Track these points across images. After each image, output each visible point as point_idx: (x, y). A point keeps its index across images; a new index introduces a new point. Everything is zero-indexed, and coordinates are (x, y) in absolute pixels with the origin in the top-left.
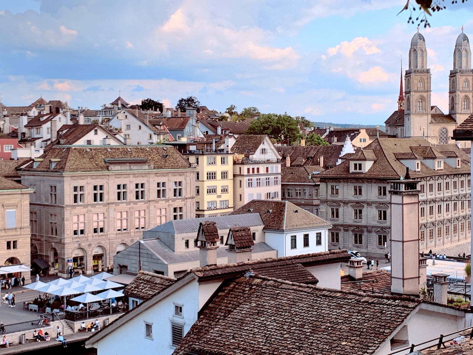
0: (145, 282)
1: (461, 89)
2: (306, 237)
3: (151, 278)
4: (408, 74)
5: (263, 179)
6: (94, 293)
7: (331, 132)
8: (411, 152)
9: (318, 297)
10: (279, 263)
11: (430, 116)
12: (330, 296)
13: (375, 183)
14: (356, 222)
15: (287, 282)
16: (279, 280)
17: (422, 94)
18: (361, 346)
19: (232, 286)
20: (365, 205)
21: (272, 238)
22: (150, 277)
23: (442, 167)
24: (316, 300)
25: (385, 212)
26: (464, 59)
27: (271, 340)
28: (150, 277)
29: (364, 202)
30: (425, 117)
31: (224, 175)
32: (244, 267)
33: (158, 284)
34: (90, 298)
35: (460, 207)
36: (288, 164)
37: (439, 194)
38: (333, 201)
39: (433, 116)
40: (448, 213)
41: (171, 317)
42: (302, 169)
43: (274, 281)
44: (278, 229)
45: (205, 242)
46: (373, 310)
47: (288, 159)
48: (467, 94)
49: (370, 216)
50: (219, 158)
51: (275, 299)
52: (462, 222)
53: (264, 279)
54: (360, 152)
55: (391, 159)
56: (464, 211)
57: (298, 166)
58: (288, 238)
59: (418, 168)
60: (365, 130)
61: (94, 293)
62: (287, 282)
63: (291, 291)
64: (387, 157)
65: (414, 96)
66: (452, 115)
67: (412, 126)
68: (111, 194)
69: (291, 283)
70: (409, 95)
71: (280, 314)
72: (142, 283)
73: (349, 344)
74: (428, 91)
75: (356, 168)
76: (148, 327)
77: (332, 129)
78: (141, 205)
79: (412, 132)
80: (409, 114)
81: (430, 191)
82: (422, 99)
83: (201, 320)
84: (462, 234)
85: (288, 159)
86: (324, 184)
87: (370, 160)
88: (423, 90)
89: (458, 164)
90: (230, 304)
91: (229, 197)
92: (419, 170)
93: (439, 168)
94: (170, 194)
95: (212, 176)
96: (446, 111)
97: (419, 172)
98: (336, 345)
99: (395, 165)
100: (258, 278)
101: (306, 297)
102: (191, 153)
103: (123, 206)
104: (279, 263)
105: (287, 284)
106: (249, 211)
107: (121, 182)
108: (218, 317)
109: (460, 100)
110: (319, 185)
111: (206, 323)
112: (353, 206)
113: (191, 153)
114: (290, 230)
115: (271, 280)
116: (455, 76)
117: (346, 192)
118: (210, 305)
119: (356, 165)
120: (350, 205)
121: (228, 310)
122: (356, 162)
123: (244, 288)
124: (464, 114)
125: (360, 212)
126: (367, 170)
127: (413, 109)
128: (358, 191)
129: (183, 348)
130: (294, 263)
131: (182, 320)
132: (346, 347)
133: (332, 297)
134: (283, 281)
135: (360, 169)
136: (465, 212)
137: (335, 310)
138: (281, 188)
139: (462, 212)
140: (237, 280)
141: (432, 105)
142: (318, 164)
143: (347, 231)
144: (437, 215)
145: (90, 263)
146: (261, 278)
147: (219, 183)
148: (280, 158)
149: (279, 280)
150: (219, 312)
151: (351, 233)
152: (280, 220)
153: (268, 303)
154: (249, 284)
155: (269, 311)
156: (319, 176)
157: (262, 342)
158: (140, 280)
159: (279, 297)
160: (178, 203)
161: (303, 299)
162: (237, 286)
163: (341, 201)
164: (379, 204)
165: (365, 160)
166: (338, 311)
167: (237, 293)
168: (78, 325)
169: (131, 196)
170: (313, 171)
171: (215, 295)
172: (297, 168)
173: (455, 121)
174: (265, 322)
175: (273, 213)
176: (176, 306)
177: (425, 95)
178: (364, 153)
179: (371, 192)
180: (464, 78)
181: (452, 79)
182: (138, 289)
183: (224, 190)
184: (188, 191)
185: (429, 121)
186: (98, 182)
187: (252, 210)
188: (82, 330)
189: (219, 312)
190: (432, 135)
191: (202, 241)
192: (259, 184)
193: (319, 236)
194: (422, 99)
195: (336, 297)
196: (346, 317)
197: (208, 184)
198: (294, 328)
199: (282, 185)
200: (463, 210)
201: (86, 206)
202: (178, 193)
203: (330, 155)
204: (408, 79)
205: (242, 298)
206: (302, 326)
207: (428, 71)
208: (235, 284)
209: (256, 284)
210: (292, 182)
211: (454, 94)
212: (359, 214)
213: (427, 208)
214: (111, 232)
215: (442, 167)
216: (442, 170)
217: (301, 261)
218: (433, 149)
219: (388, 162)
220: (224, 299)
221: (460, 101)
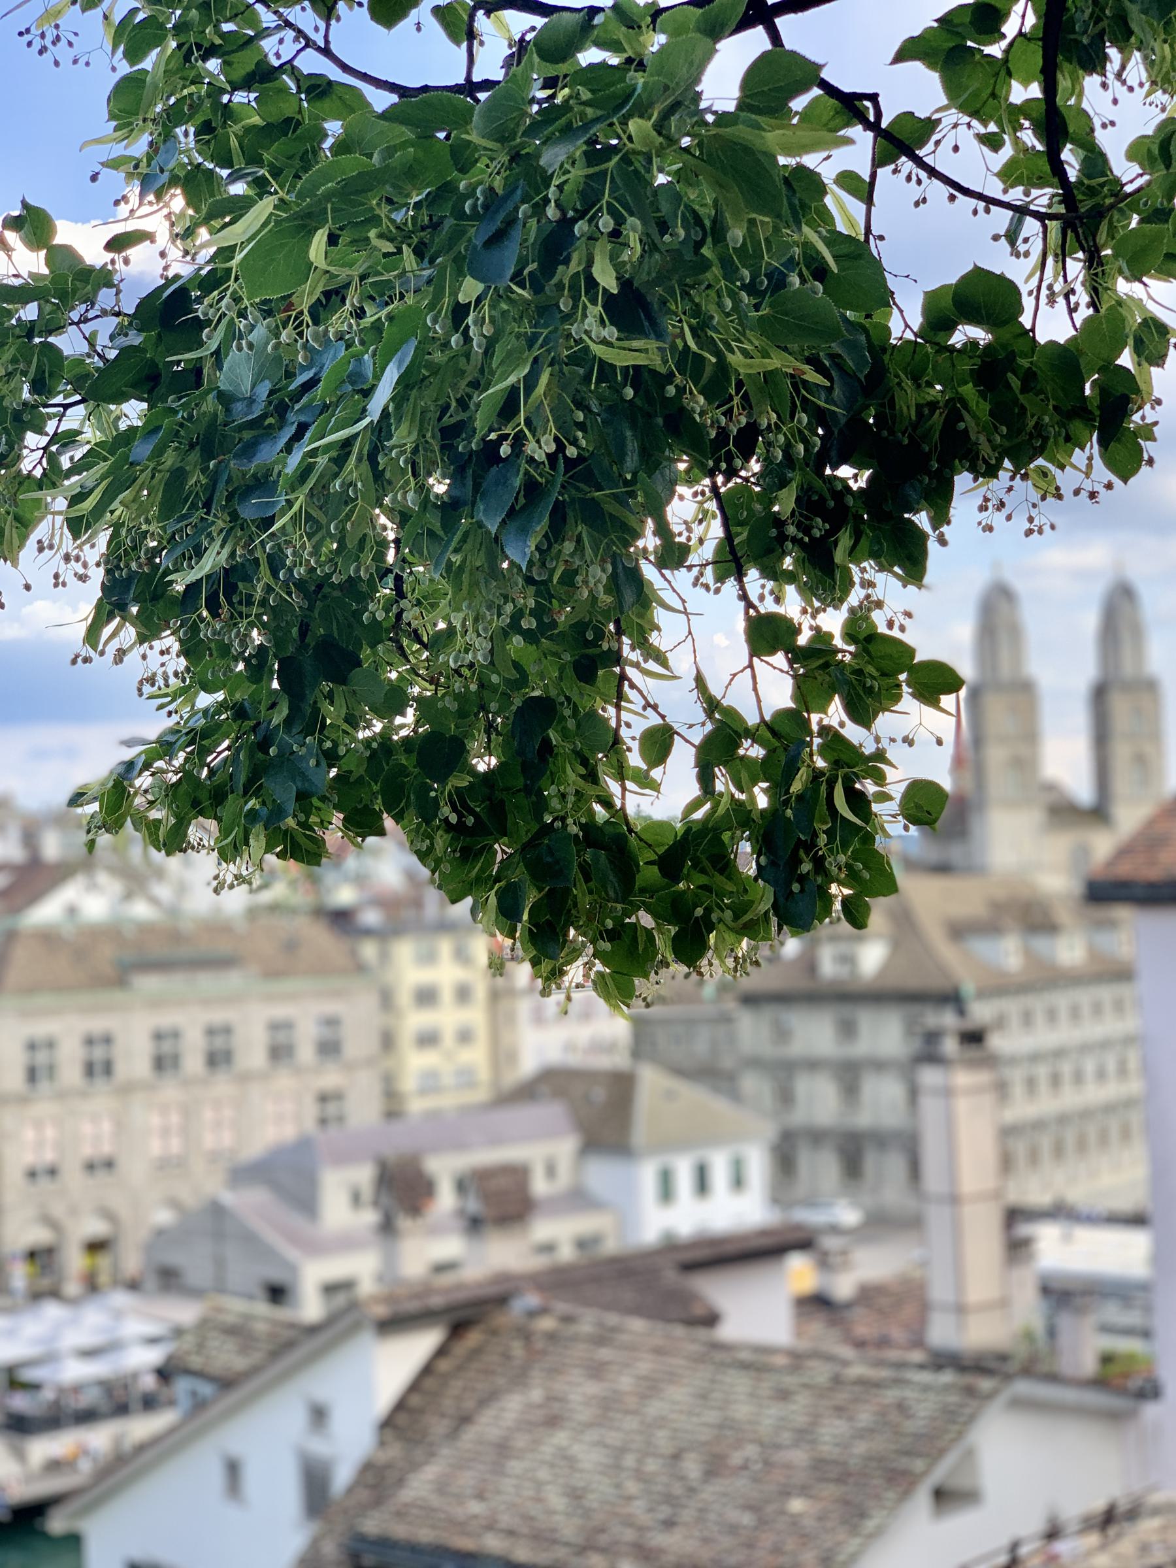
6: (89, 1353)
21: (601, 1175)
31: (463, 994)
34: (74, 1371)
49: (882, 1101)
50: (445, 947)
61: (89, 1353)
65: (996, 755)
68: (134, 1058)
76: (233, 1469)
78: (223, 1086)
91: (476, 1056)
94: (306, 1053)
95: (426, 997)
99: (948, 953)
102: (368, 932)
103: (170, 1092)
107: (167, 1019)
113: (368, 932)
117: (814, 1033)
128: (847, 1030)
145: (75, 1262)
147: (447, 1018)
153: (580, 1391)
160: (331, 1079)
168: (43, 1448)
169: (193, 1063)
171: (427, 1370)
179: (885, 1034)
183: (465, 1037)
184: (359, 1042)
186: (98, 1024)
188: (54, 1466)
197: (415, 1020)
201: (61, 1096)
202: (329, 1048)
206: (676, 1457)
213: (1042, 1072)
214: (136, 1169)
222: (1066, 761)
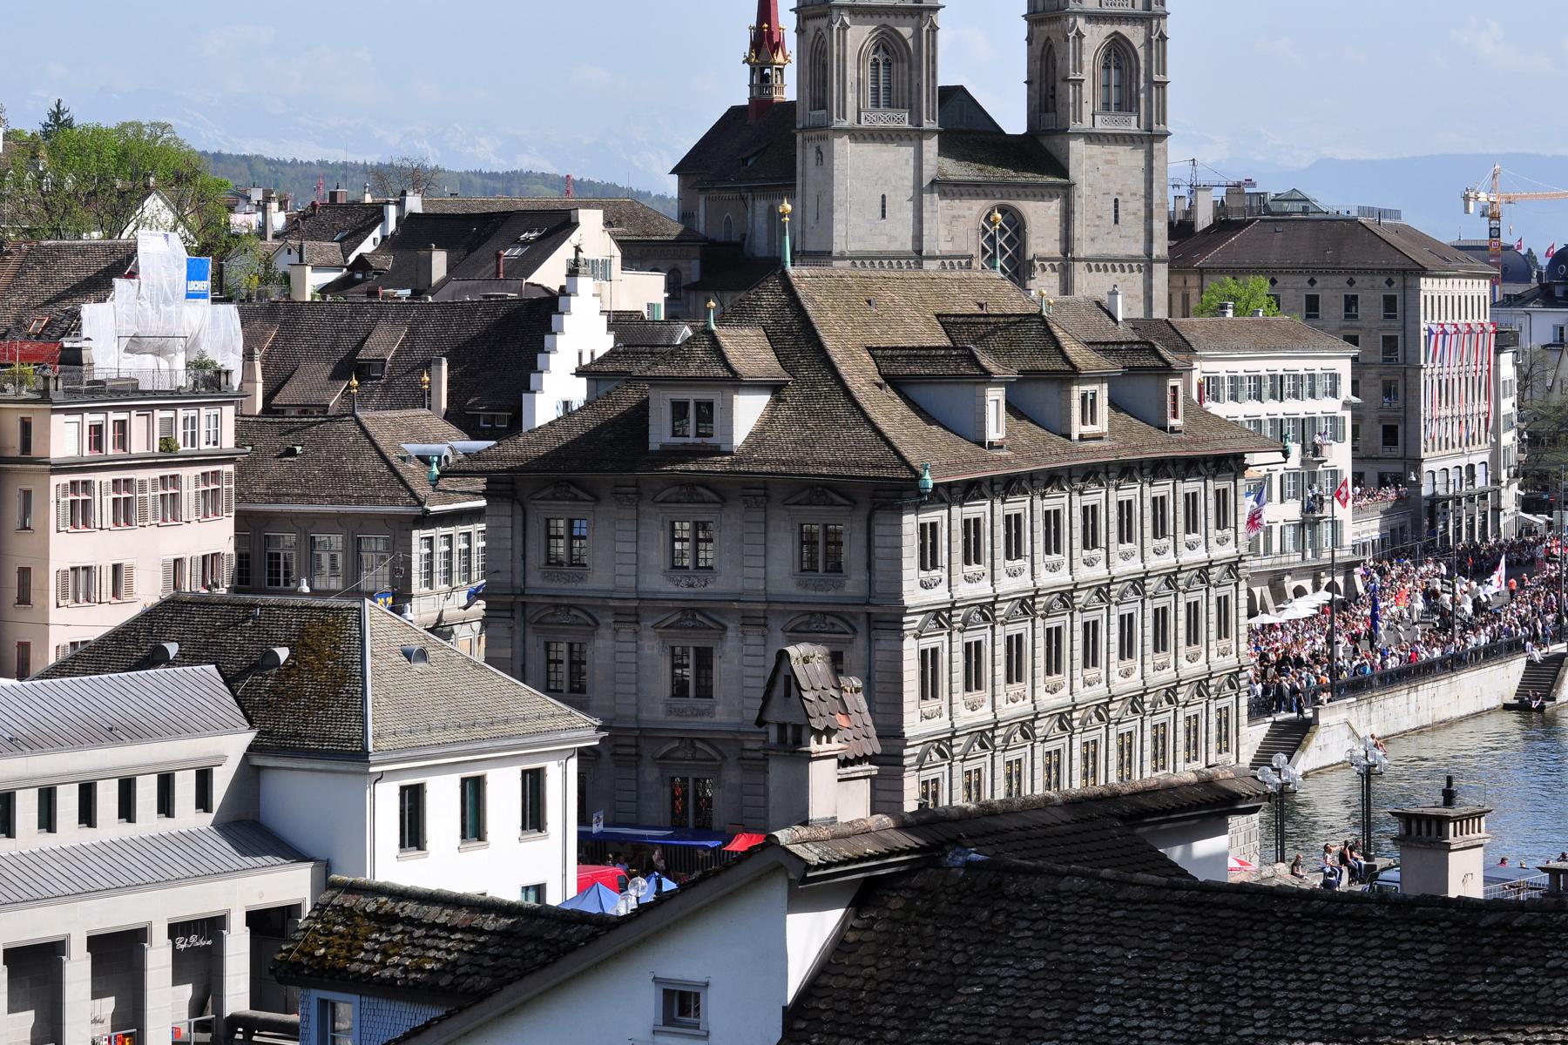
2: (473, 792)
5: (142, 483)
8: (946, 342)
11: (931, 146)
13: (784, 503)
14: (680, 712)
15: (1140, 876)
24: (1293, 933)
40: (1128, 663)
48: (1125, 29)
52: (1191, 711)
55: (860, 376)
56: (1198, 655)
57: (305, 410)
58: (386, 802)
62: (1140, 876)
63: (1178, 909)
66: (1045, 142)
67: (839, 194)
70: (822, 22)
77: (414, 204)
79: (839, 229)
80: (824, 131)
81: (1048, 552)
86: (507, 509)
87: (756, 386)
89: (1175, 406)
93: (1089, 429)
96: (1012, 117)
106: (156, 658)
109: (1088, 58)
112: (663, 629)
114: (396, 754)
115: (1068, 874)
119: (679, 409)
122: (680, 395)
125: (704, 659)
126: (740, 436)
141: (944, 80)
144: (1077, 674)
151: (651, 774)
173: (1064, 173)
176: (668, 994)
178: (725, 342)
187: (173, 649)
190: (945, 247)
191: (782, 727)
192: (125, 513)
193: (533, 784)
196: (1441, 982)
199: (242, 520)
200: (1194, 648)
210: (301, 498)
215: (1102, 425)
216: (1099, 438)
218: (1059, 333)
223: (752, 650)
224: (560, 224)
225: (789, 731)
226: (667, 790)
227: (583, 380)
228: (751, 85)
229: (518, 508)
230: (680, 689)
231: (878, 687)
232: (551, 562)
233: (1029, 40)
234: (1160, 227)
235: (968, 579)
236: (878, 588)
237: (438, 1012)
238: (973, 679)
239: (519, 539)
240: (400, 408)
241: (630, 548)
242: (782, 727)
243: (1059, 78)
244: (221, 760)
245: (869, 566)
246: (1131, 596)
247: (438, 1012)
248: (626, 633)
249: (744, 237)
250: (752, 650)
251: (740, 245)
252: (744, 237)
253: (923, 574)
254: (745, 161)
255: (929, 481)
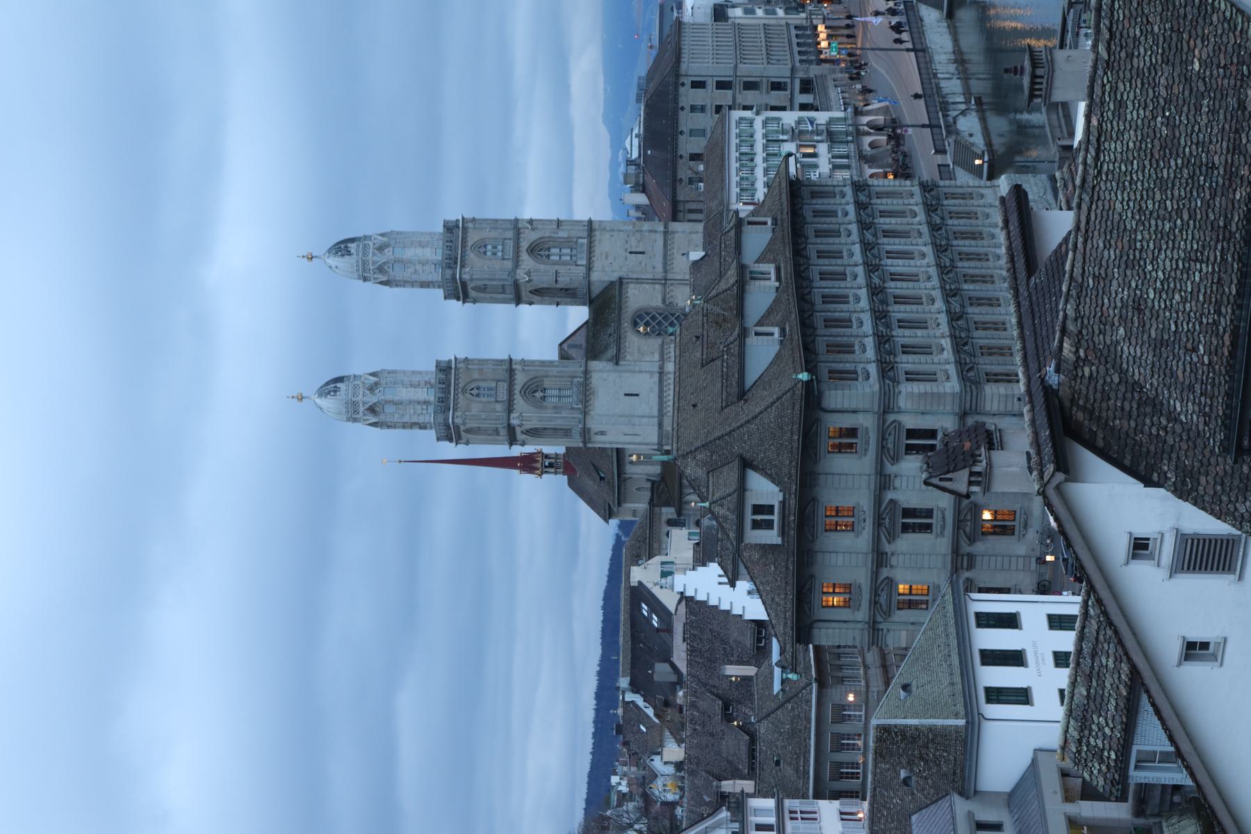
0: (1086, 732)
1: (509, 265)
3: (1075, 719)
4: (451, 434)
7: (635, 687)
9: (1100, 172)
10: (1027, 323)
11: (594, 365)
12: (1098, 140)
14: (943, 528)
15: (1068, 267)
16: (1064, 289)
17: (518, 388)
18: (1200, 20)
19: (1080, 416)
20: (890, 495)
22: (1072, 722)
23: (770, 268)
24: (1107, 175)
25: (912, 433)
26: (409, 253)
27: (1197, 251)
28: (1072, 722)
29: (878, 501)
30: (596, 379)
32: (1034, 390)
33: (1088, 692)
35: (899, 220)
36: (748, 786)
37: (855, 277)
38: (874, 603)
39: (593, 353)
41: (1163, 573)
42: (763, 729)
43: (1066, 302)
44: (965, 742)
45: (972, 474)
46: (1126, 22)
47: (728, 786)
48: (525, 245)
51: (1107, 278)
53: (1064, 331)
54: (717, 509)
57: (752, 754)
59: (772, 334)
60: (634, 569)
62: (1068, 267)
63: (1089, 246)
64: (734, 425)
66: (594, 295)
69: (1070, 255)
70: (518, 430)
71: (1141, 252)
72: (1088, 744)
73: (1197, 52)
74: (510, 367)
75: (769, 525)
77: (624, 682)
81: (848, 303)
82: (534, 390)
83: (1162, 476)
84: (987, 216)
85: (728, 786)
86: (815, 632)
88: (506, 385)
90: (1123, 409)
92: (776, 330)
93: (773, 276)
96: (578, 315)
97: (783, 331)
98: (1200, 83)
100: (1061, 348)
101: (1100, 203)
104: (1027, 323)
105: (1073, 266)
108: (1154, 431)
110: (816, 648)
111: (1170, 459)
112: (892, 538)
116: (464, 284)
117: (845, 557)
118: (1127, 462)
119: (757, 525)
120: (888, 548)
121: (1138, 409)
122: (748, 524)
123: (1086, 381)
124: (590, 259)
125: (908, 512)
126: (774, 488)
127: (567, 418)
128: (844, 519)
129: (1231, 507)
130: (1026, 294)
131: (1167, 536)
132: (1204, 57)
133: (1100, 136)
134: (1067, 275)
135: (769, 509)
136: (915, 208)
137: (1129, 117)
138: (826, 802)
139: (915, 215)
140: (1067, 404)
141: (552, 355)
142: (746, 680)
143: (971, 557)
146: (1061, 342)
148: (724, 814)
149: (1064, 289)
150: (1142, 432)
151: (979, 547)
152: (936, 737)
154: (1076, 368)
155: (1133, 285)
156: (788, 647)
157: (1200, 271)
158: (1079, 752)
159: (1102, 272)
161: (1107, 207)
162: (1081, 402)
163: (875, 574)
164: (886, 454)
165: (742, 488)
166: (1130, 107)
167: (1099, 395)
170: (771, 694)
172: (761, 746)
174: (1158, 284)
175: (910, 764)
176: (1134, 557)
177: (520, 379)
178: (717, 496)
179: (848, 480)
180: (472, 256)
181: (472, 294)
182: (1103, 750)
185: (610, 366)
189: (1142, 432)
190: (657, 357)
191: (970, 483)
193: (987, 620)
194: (534, 390)
195: (1100, 124)
196: (1142, 84)
198: (1168, 203)
199: (818, 795)
203: (717, 644)
204: (467, 431)
205: (1109, 380)
207: (444, 369)
208: (1075, 409)
209: (1074, 349)
210: (807, 760)
211: (523, 288)
212: (915, 517)
213: (899, 312)
216: (778, 269)
217: (1024, 282)
219: (748, 422)
220: (1113, 429)
221: (548, 267)
222: (537, 332)
223: (904, 484)
224: (640, 594)
225: (973, 479)
226: (990, 537)
227: (738, 583)
228: (556, 473)
229: (816, 625)
230: (927, 528)
231: (928, 408)
232: (847, 604)
233: (531, 303)
234: (646, 226)
235: (864, 351)
236: (867, 406)
237: (1144, 697)
238: (924, 350)
239: (834, 625)
240: (752, 695)
241: (840, 557)
242: (970, 483)
243: (554, 285)
244: (970, 814)
245: (854, 412)
246: (875, 251)
247: (1144, 697)
248: (894, 561)
249: (648, 480)
250: (904, 484)
251: (653, 483)
252: (648, 480)
253: (860, 379)
254: (602, 478)
255: (804, 376)
